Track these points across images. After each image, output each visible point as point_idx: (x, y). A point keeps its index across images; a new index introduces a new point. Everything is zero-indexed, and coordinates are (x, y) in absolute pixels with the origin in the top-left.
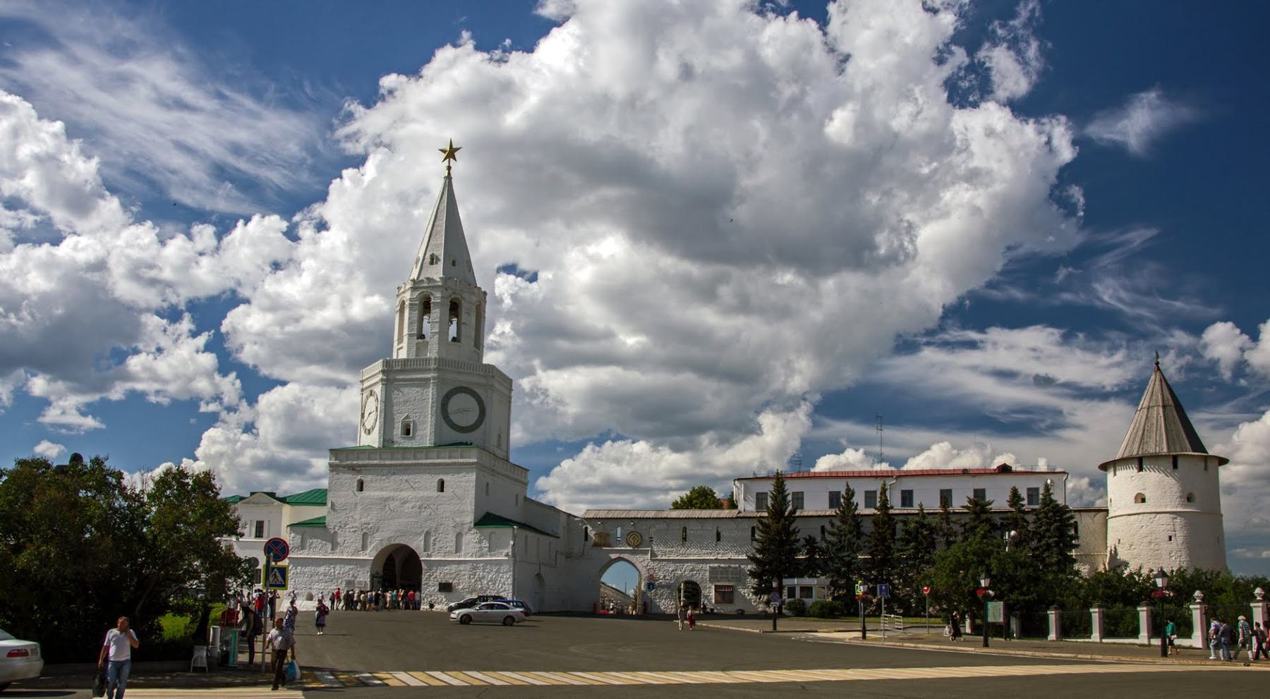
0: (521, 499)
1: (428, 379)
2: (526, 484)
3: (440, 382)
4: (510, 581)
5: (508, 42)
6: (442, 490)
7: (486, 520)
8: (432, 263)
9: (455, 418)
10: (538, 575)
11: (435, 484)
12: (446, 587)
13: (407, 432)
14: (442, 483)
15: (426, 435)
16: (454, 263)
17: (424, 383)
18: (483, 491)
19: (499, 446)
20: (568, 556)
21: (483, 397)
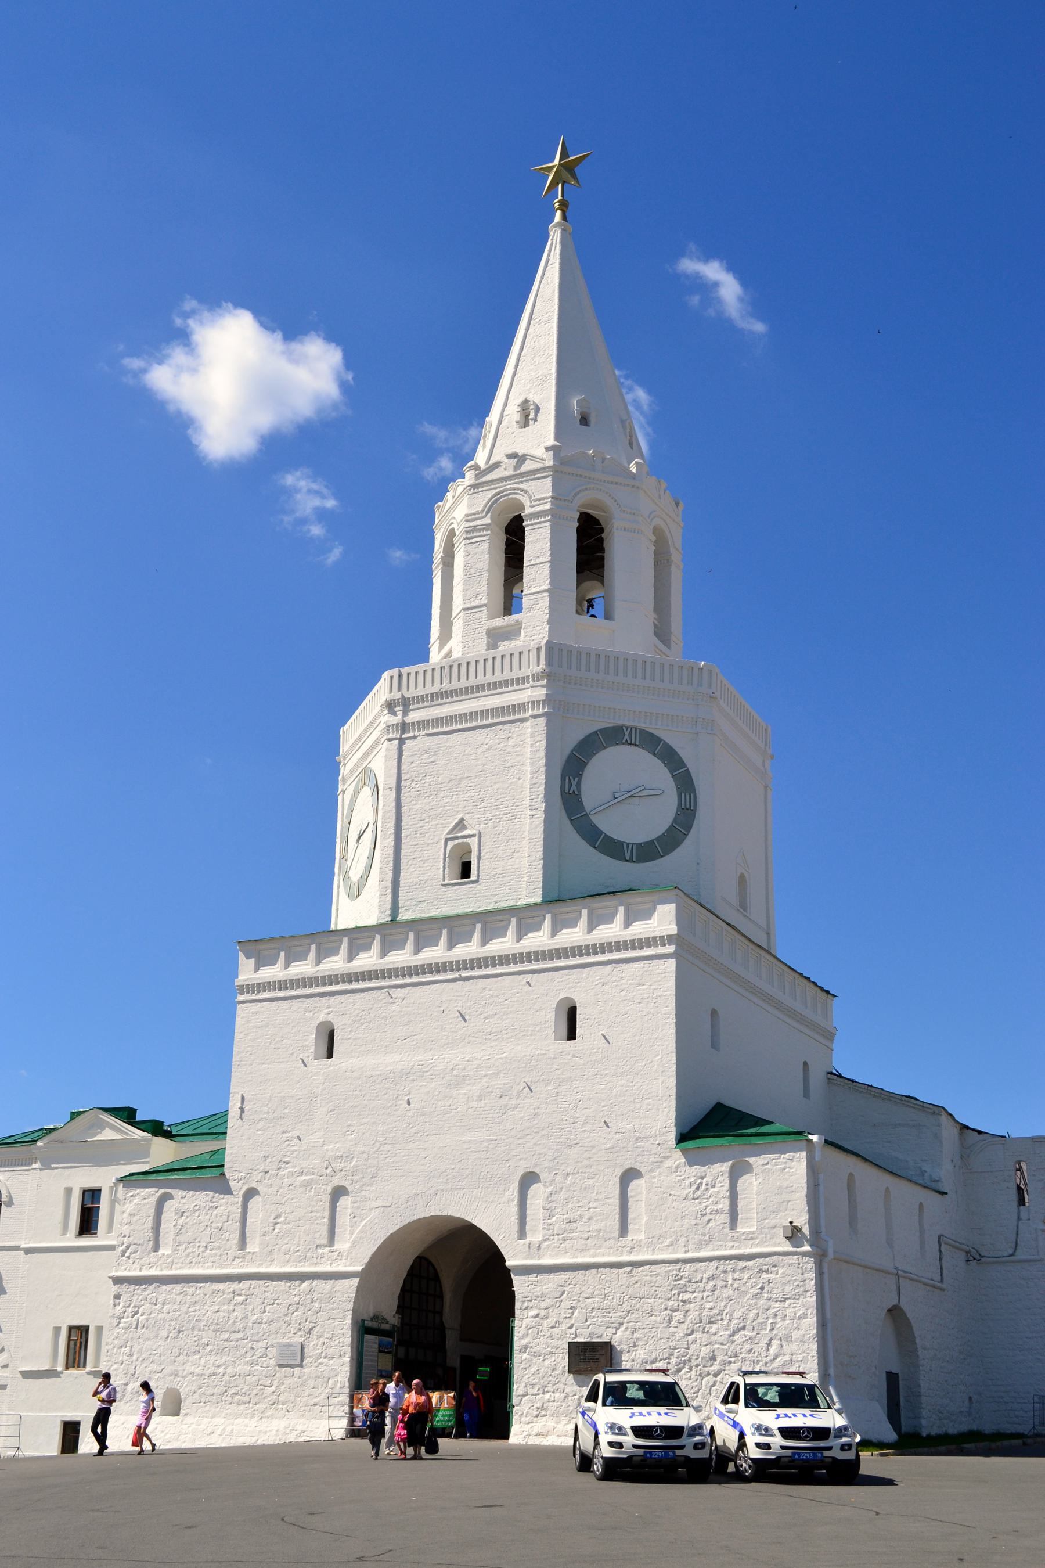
0: (817, 1076)
1: (520, 707)
2: (830, 1036)
3: (557, 710)
4: (810, 1324)
5: (695, 300)
6: (572, 1035)
7: (713, 1124)
8: (525, 420)
9: (609, 824)
10: (895, 1312)
11: (550, 1020)
12: (589, 1357)
13: (465, 870)
14: (572, 1014)
15: (515, 867)
16: (584, 420)
17: (511, 714)
18: (699, 1031)
19: (743, 905)
20: (973, 1257)
21: (685, 753)
